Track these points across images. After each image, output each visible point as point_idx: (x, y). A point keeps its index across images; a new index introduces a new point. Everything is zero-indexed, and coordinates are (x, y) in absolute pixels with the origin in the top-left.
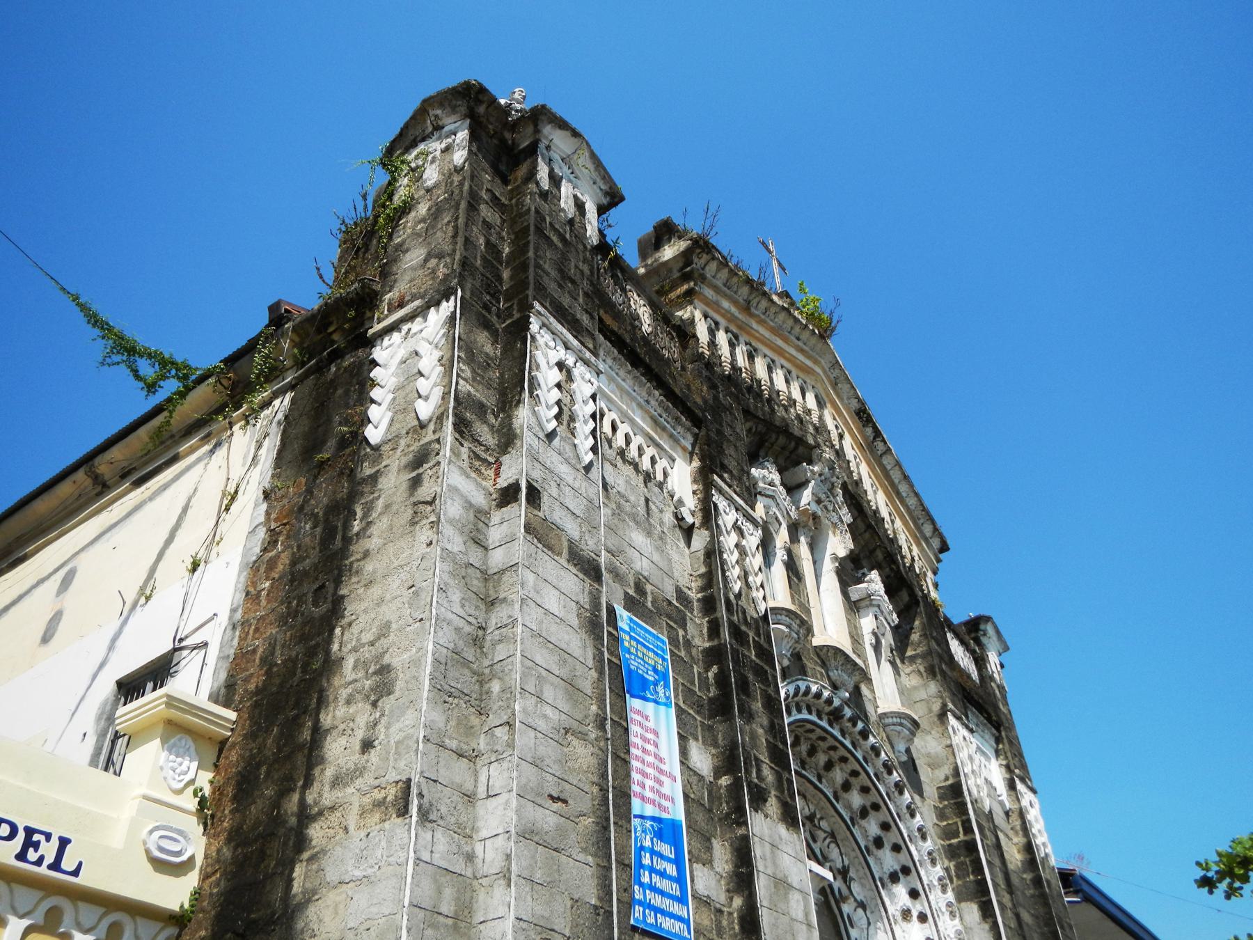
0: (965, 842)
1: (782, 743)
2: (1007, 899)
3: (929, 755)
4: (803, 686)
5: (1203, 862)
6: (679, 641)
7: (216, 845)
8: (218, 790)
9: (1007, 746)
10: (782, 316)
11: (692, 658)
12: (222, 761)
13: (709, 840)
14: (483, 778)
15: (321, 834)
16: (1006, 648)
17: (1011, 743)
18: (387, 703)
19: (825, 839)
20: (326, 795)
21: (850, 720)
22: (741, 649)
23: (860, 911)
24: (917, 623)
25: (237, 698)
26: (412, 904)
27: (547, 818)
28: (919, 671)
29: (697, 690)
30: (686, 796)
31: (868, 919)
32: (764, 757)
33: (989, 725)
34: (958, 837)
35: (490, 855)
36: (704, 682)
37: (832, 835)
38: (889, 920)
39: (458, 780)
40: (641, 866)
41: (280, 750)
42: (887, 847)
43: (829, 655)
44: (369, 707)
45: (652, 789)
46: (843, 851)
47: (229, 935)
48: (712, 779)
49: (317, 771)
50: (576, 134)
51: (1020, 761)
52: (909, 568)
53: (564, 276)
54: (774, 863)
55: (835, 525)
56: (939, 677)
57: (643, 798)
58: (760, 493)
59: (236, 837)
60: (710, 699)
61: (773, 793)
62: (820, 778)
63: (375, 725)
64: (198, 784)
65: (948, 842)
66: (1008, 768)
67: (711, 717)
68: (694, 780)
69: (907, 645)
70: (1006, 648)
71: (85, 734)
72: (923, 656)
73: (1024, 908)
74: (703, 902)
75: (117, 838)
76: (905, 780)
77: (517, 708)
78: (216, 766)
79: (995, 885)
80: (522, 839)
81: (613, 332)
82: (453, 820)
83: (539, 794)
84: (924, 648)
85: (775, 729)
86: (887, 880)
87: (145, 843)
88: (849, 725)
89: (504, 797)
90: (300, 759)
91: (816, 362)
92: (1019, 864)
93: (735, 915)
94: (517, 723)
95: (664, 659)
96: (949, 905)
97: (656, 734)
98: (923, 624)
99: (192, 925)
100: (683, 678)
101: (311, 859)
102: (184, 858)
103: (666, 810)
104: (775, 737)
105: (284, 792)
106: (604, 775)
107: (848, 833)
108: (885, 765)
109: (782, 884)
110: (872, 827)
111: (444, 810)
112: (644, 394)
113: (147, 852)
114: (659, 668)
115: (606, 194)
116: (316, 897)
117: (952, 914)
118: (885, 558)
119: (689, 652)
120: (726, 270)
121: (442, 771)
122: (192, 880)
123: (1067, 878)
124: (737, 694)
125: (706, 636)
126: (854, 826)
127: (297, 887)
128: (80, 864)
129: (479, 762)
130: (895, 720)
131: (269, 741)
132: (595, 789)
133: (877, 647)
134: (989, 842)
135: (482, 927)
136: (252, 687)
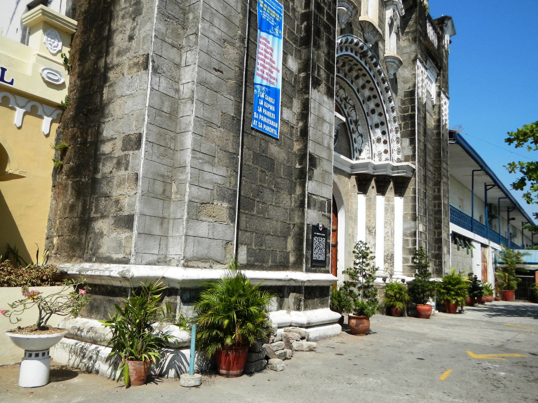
0: (411, 114)
1: (332, 61)
2: (422, 138)
3: (404, 78)
4: (350, 39)
5: (510, 132)
6: (289, 8)
7: (74, 79)
8: (72, 56)
9: (442, 78)
11: (295, 17)
12: (73, 43)
13: (292, 99)
14: (184, 58)
15: (113, 76)
16: (454, 34)
17: (444, 77)
18: (139, 19)
19: (350, 108)
20: (115, 59)
21: (370, 57)
22: (319, 15)
23: (360, 137)
24: (414, 16)
25: (77, 15)
26: (149, 106)
27: (213, 78)
28: (409, 39)
29: (295, 32)
30: (283, 79)
31: (363, 141)
32: (322, 66)
33: (436, 68)
34: (408, 112)
35: (186, 90)
36: (299, 30)
37: (354, 107)
38: (371, 142)
39: (172, 57)
40: (259, 105)
41: (96, 39)
42: (377, 113)
43: (367, 26)
44: (131, 21)
45: (267, 74)
46: (357, 113)
47: (81, 114)
48: (297, 74)
49: (111, 49)
51: (446, 85)
54: (319, 111)
56: (417, 42)
57: (263, 77)
59: (81, 76)
60: (301, 38)
61: (324, 82)
62: (352, 82)
63: (134, 29)
64: (63, 52)
65: (403, 114)
66: (439, 87)
67: (301, 46)
68: (288, 73)
69: (406, 26)
70: (454, 34)
71: (17, 29)
72: (413, 32)
73: (430, 143)
74: (285, 122)
75: (29, 72)
76: (390, 87)
77: (200, 26)
78: (71, 45)
79: (419, 132)
80: (199, 85)
82: (169, 74)
83: (208, 67)
84: (414, 29)
85: (330, 55)
86: (373, 127)
87: (41, 74)
88: (370, 60)
89: (192, 66)
90: (104, 44)
92: (433, 126)
93: (299, 129)
94: (200, 34)
95: (280, 15)
96: (397, 138)
97: (272, 50)
98: (416, 16)
99: (67, 110)
100: (289, 26)
101: (110, 86)
102: (60, 82)
103: (273, 83)
104: (329, 58)
105: (99, 58)
106: (242, 63)
107: (361, 106)
108: (382, 79)
109: (321, 119)
110: (372, 105)
111: (165, 69)
113: (43, 78)
114: (277, 19)
116: (113, 101)
117: (398, 142)
119: (294, 14)
121: (164, 52)
122: (65, 93)
123: (452, 134)
124: (314, 36)
125: (303, 7)
126: (364, 104)
127: (105, 97)
128: (13, 80)
129: (183, 51)
130: (391, 60)
131: (92, 35)
132: (237, 69)
133: (391, 26)
134: (421, 116)
135: (181, 118)
136: (83, 10)
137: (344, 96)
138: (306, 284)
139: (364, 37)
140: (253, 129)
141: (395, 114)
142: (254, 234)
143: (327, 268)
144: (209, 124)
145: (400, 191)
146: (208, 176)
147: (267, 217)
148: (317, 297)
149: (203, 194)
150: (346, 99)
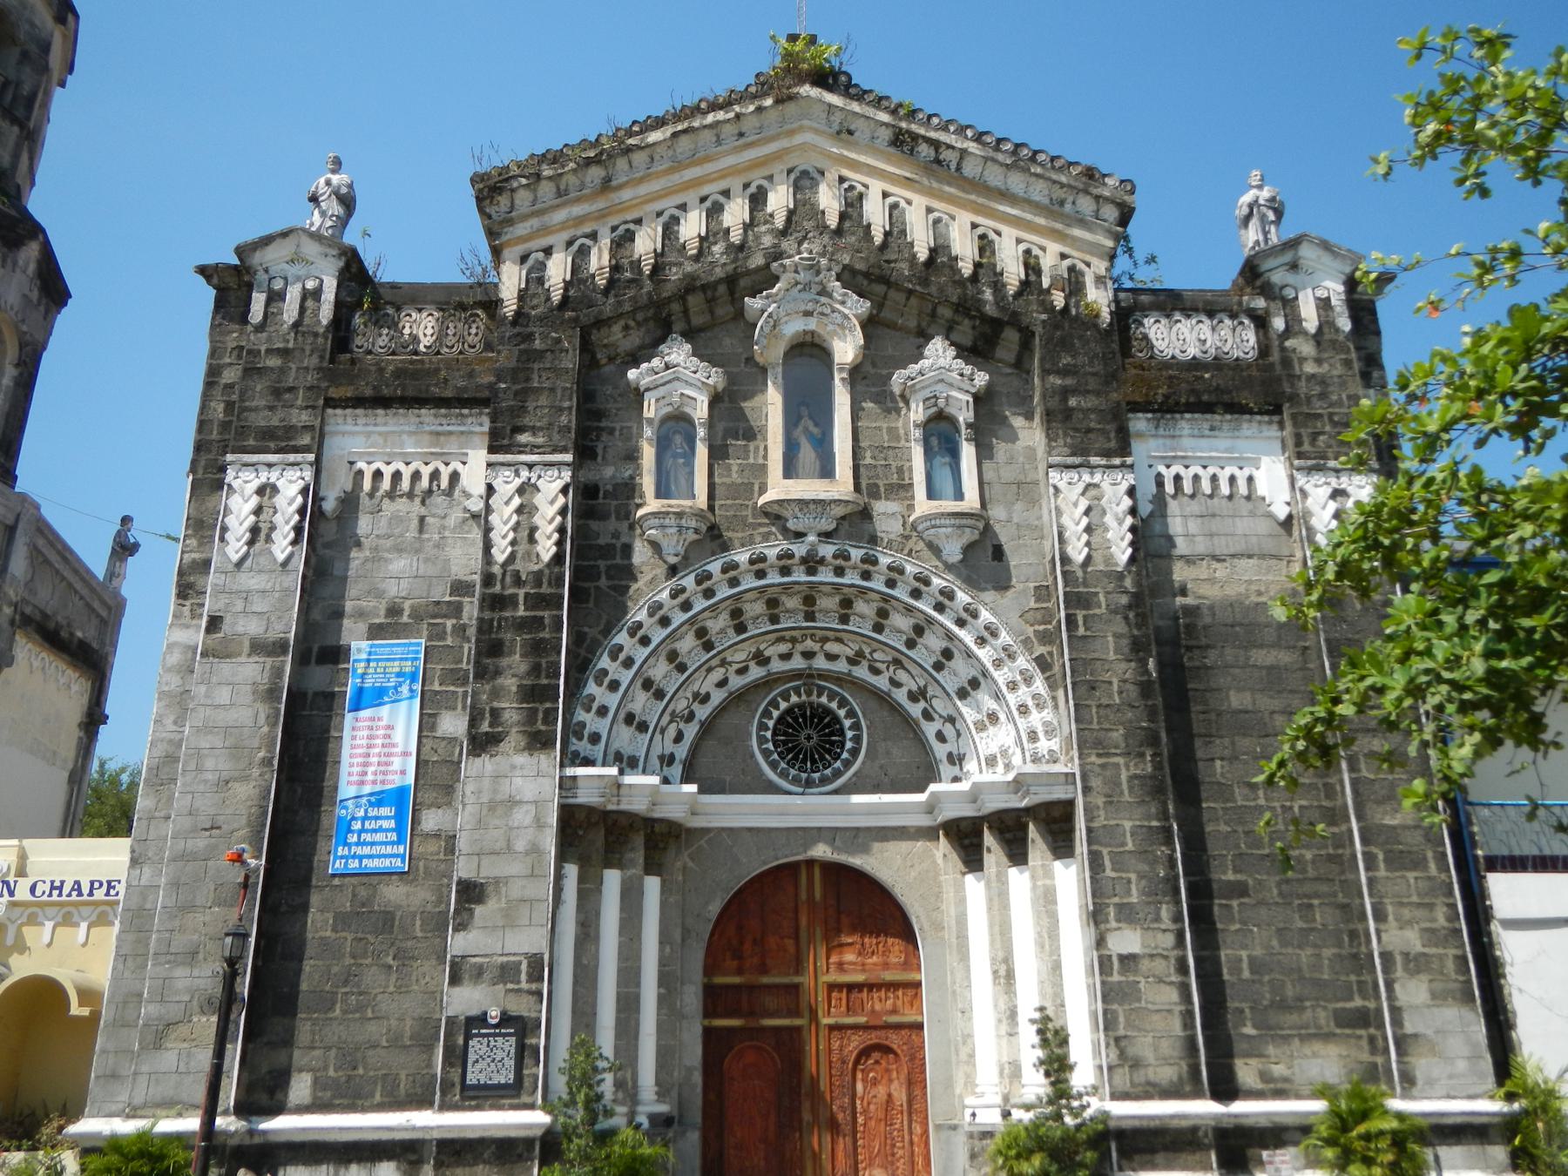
1: (548, 677)
10: (685, 143)
23: (948, 725)
37: (897, 663)
50: (285, 234)
52: (1018, 295)
53: (277, 392)
55: (842, 326)
58: (648, 390)
61: (514, 730)
81: (348, 399)
91: (791, 133)
96: (1035, 696)
106: (266, 797)
112: (414, 420)
115: (340, 255)
117: (1040, 706)
118: (956, 311)
120: (544, 183)
137: (850, 653)
138: (436, 1135)
139: (785, 531)
140: (334, 875)
141: (1005, 637)
142: (333, 1052)
143: (525, 1099)
144: (187, 908)
145: (1062, 846)
146: (180, 984)
147: (370, 1015)
148: (485, 1162)
149: (174, 1011)
150: (860, 654)
